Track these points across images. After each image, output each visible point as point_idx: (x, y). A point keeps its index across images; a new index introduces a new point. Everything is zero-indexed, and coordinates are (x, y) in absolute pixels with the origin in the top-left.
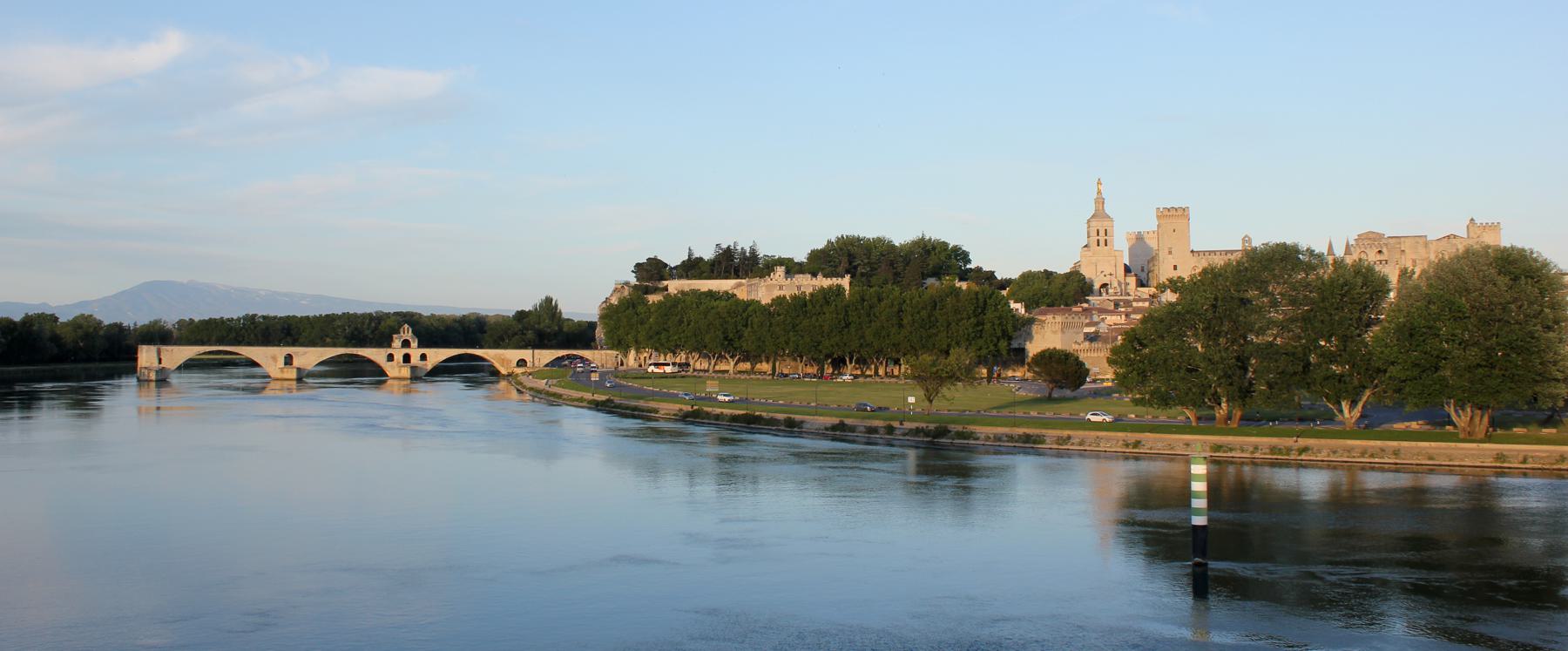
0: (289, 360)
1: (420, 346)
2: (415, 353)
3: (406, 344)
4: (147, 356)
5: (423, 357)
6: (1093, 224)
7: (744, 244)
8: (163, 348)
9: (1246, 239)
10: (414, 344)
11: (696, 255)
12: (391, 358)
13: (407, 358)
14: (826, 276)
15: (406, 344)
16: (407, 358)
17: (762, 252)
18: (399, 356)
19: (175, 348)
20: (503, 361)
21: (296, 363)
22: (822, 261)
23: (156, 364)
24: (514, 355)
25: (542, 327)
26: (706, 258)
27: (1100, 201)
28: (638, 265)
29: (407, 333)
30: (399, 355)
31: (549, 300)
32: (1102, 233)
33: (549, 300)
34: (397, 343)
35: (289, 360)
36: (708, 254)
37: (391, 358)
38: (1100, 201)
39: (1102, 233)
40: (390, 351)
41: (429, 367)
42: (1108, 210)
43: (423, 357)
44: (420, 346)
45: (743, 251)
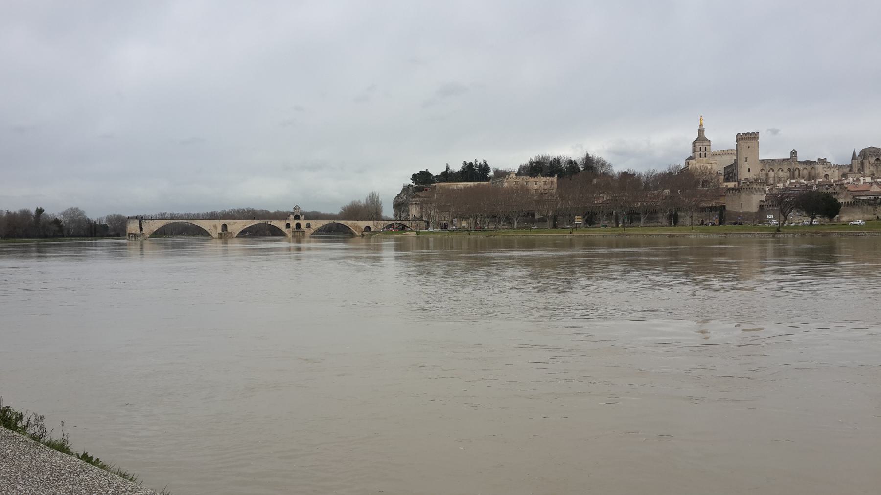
0: (225, 226)
5: (309, 226)
6: (698, 144)
9: (794, 153)
12: (288, 226)
18: (293, 224)
20: (356, 227)
21: (229, 229)
23: (138, 232)
25: (368, 210)
27: (701, 131)
28: (414, 176)
32: (703, 149)
35: (225, 226)
37: (288, 226)
38: (701, 131)
39: (703, 149)
40: (287, 222)
42: (707, 135)
43: (309, 226)
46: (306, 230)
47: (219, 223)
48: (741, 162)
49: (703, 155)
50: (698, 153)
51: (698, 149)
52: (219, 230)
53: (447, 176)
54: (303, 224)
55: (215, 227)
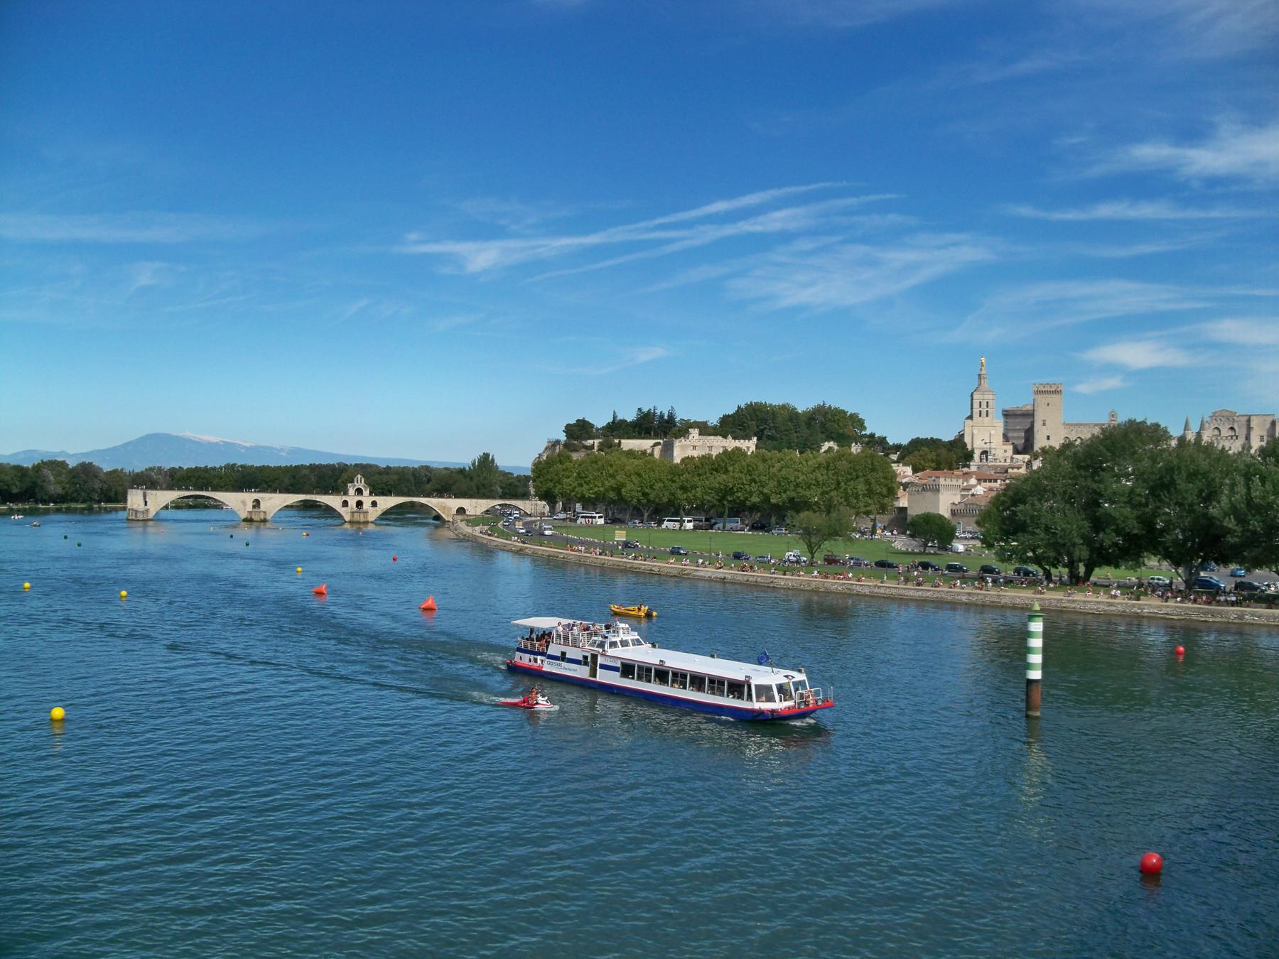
1: (371, 494)
2: (367, 500)
3: (359, 492)
4: (135, 499)
5: (374, 504)
7: (663, 409)
8: (149, 492)
10: (366, 492)
11: (620, 417)
12: (345, 504)
13: (359, 504)
14: (734, 438)
15: (359, 492)
16: (359, 504)
17: (680, 415)
19: (159, 493)
22: (733, 425)
24: (454, 503)
25: (480, 479)
26: (629, 419)
28: (568, 426)
29: (360, 482)
30: (352, 500)
31: (486, 456)
32: (984, 405)
33: (486, 456)
34: (352, 491)
36: (630, 416)
37: (345, 504)
39: (984, 405)
40: (345, 498)
41: (380, 513)
43: (374, 504)
44: (371, 494)
45: (662, 416)
46: (371, 510)
47: (249, 497)
48: (1038, 426)
49: (984, 414)
50: (976, 411)
51: (976, 405)
52: (250, 507)
53: (618, 428)
54: (367, 500)
55: (244, 503)
